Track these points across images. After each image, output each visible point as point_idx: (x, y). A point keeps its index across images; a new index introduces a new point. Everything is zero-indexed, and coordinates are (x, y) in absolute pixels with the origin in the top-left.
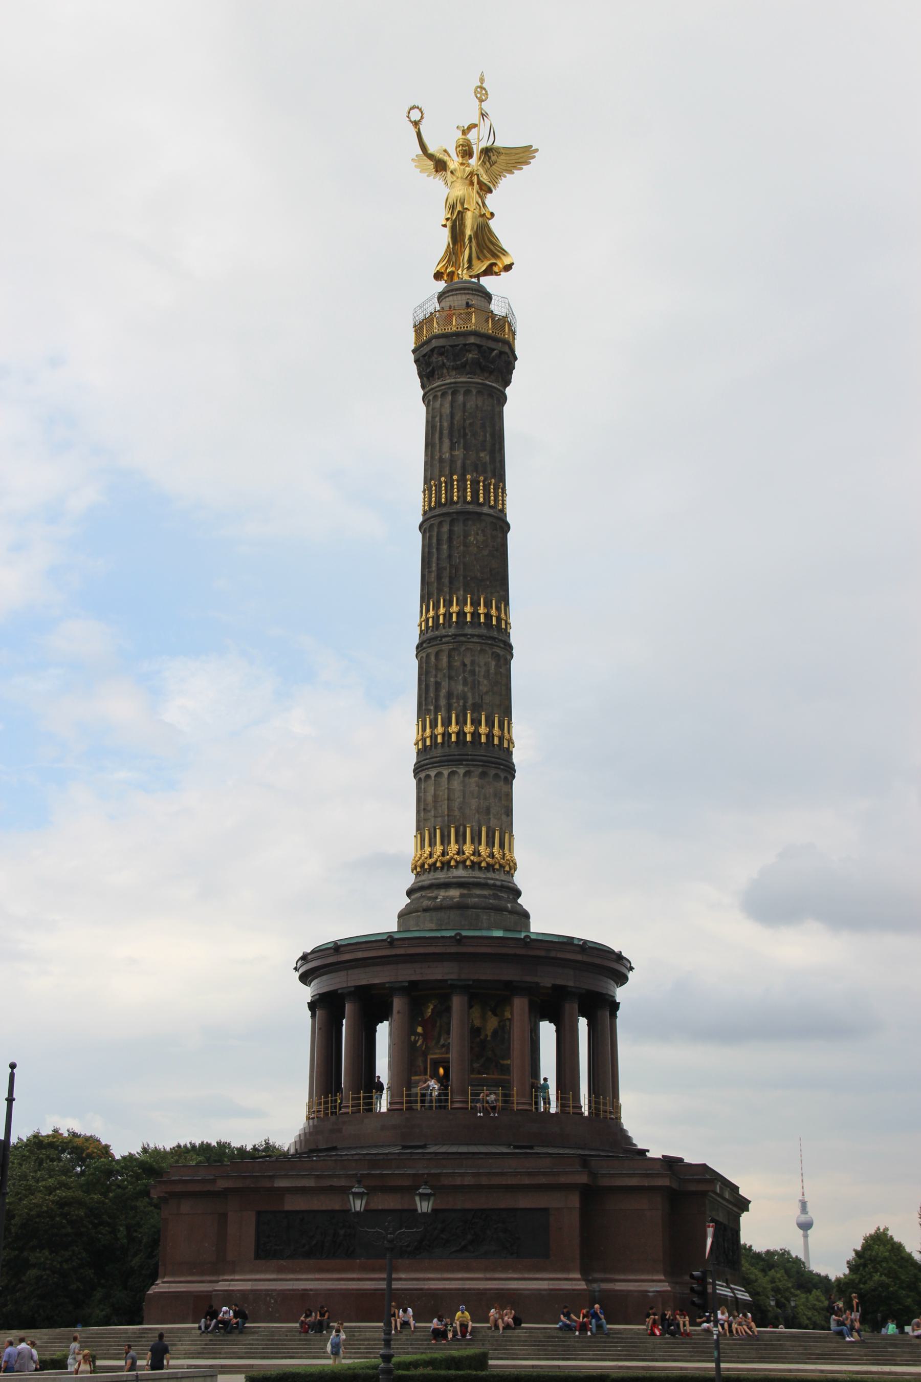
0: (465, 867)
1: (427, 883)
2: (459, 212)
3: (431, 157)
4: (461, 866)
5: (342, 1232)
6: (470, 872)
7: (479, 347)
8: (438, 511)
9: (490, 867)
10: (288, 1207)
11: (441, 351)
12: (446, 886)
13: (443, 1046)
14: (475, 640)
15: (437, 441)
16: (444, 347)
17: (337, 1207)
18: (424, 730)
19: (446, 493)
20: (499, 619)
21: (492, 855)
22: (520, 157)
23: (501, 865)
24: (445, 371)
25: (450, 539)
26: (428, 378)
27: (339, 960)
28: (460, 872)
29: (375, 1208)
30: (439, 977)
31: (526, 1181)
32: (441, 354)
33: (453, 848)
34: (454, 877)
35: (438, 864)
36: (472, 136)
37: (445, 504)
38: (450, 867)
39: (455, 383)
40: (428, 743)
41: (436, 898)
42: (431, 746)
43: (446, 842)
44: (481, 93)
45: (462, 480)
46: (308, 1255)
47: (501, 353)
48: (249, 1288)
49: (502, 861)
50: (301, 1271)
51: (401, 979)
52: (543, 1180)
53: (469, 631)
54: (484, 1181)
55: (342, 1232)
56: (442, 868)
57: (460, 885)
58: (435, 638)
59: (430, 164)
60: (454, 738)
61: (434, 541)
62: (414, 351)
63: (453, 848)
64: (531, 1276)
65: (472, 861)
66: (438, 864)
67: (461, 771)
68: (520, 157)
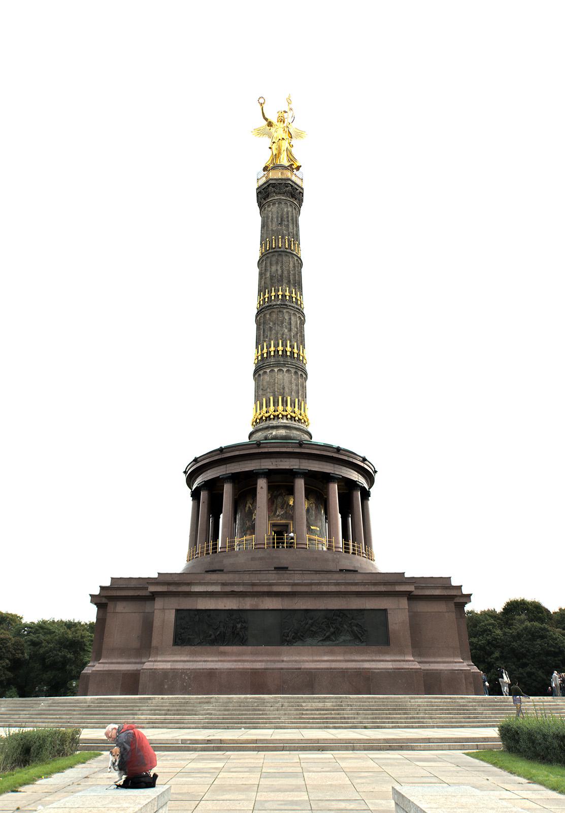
0: (287, 419)
2: (279, 139)
3: (266, 119)
4: (285, 418)
5: (239, 626)
6: (290, 421)
7: (292, 186)
9: (299, 420)
11: (274, 185)
13: (278, 516)
14: (291, 308)
15: (270, 223)
16: (275, 184)
17: (235, 608)
18: (262, 350)
19: (275, 244)
20: (301, 301)
21: (301, 414)
22: (300, 135)
23: (305, 421)
24: (274, 194)
26: (265, 199)
27: (223, 457)
28: (285, 421)
29: (263, 608)
30: (287, 467)
32: (273, 187)
33: (280, 408)
34: (281, 423)
35: (272, 417)
36: (286, 115)
37: (274, 249)
38: (279, 418)
39: (280, 199)
40: (265, 355)
41: (272, 433)
42: (267, 358)
43: (276, 405)
44: (289, 101)
45: (283, 238)
47: (300, 192)
48: (169, 667)
49: (305, 419)
51: (263, 467)
53: (286, 303)
54: (343, 588)
55: (239, 626)
56: (274, 419)
57: (286, 427)
59: (266, 123)
60: (280, 353)
61: (269, 264)
62: (257, 189)
63: (280, 408)
64: (378, 658)
65: (291, 416)
66: (272, 417)
67: (285, 370)
68: (300, 135)
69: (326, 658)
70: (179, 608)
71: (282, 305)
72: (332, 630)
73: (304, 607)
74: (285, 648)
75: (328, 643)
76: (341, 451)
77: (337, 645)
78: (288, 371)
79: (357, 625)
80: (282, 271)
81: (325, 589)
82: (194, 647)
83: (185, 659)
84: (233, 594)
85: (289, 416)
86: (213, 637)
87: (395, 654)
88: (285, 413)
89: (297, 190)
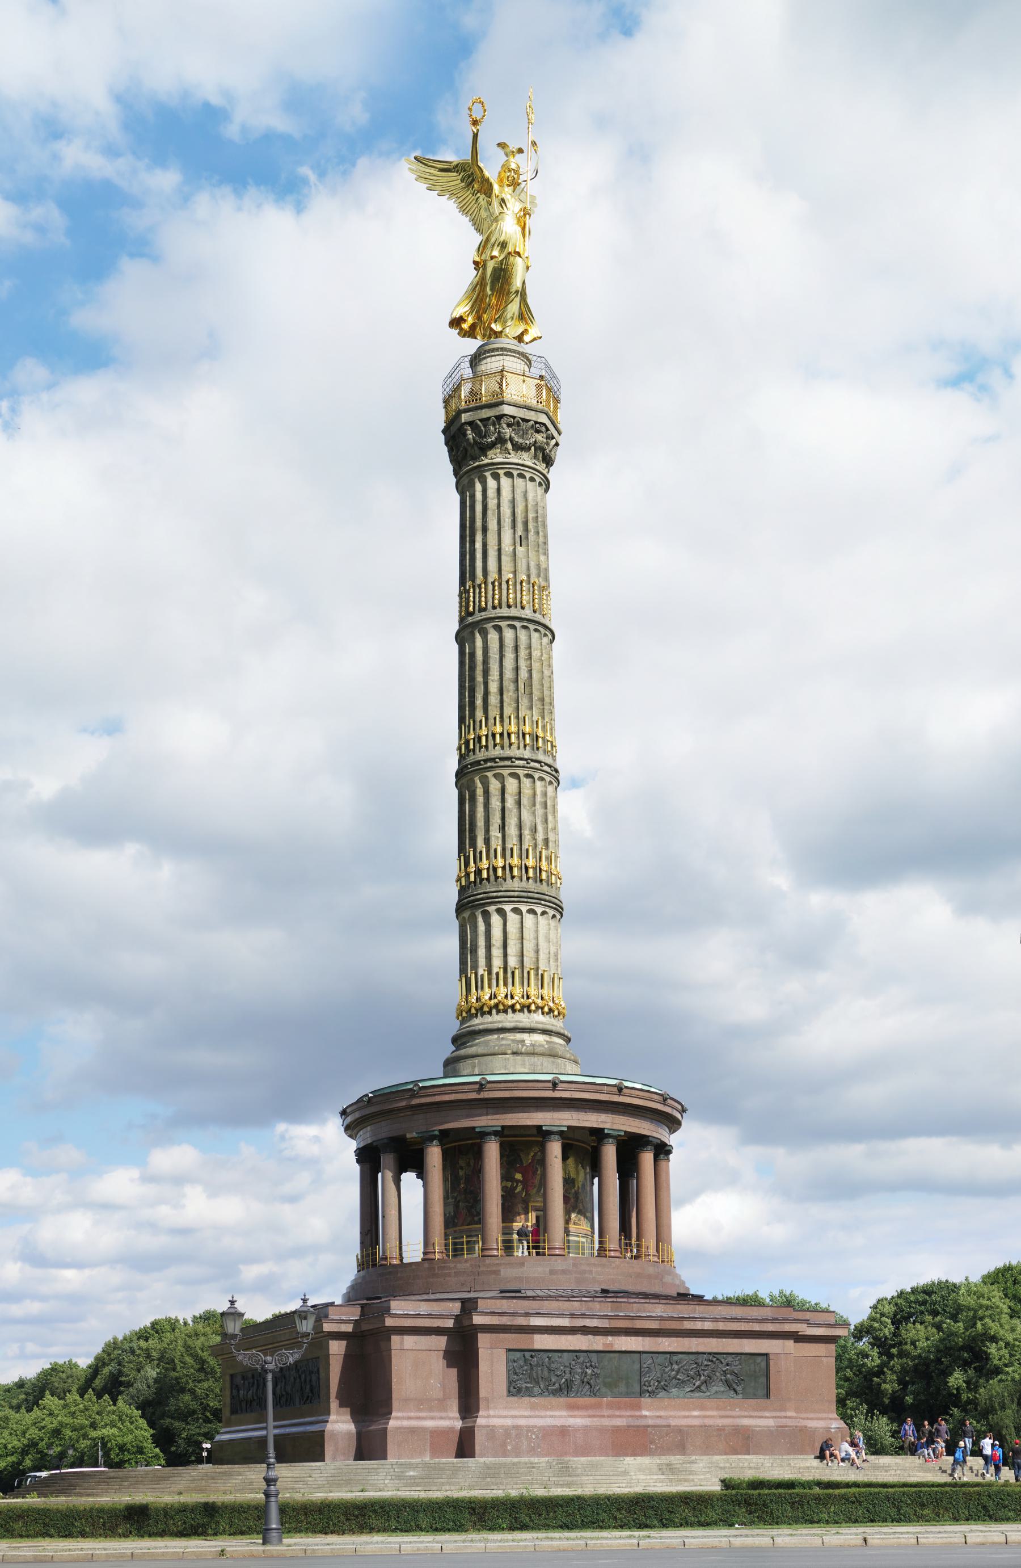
0: (543, 1013)
1: (508, 1025)
5: (589, 1371)
8: (504, 612)
10: (537, 1347)
12: (531, 1030)
17: (584, 1348)
25: (516, 648)
31: (756, 1327)
46: (557, 1392)
50: (552, 1409)
52: (770, 1327)
53: (541, 757)
54: (721, 1326)
56: (521, 1010)
58: (509, 759)
69: (695, 1413)
70: (511, 1347)
71: (532, 761)
72: (703, 1378)
73: (670, 1349)
74: (646, 1401)
75: (697, 1394)
76: (669, 1101)
77: (709, 1397)
78: (544, 913)
79: (733, 1373)
80: (530, 672)
81: (699, 1326)
82: (533, 1399)
83: (526, 1413)
84: (585, 1331)
85: (546, 1009)
86: (557, 1385)
87: (775, 1410)
88: (539, 1002)
89: (553, 438)
